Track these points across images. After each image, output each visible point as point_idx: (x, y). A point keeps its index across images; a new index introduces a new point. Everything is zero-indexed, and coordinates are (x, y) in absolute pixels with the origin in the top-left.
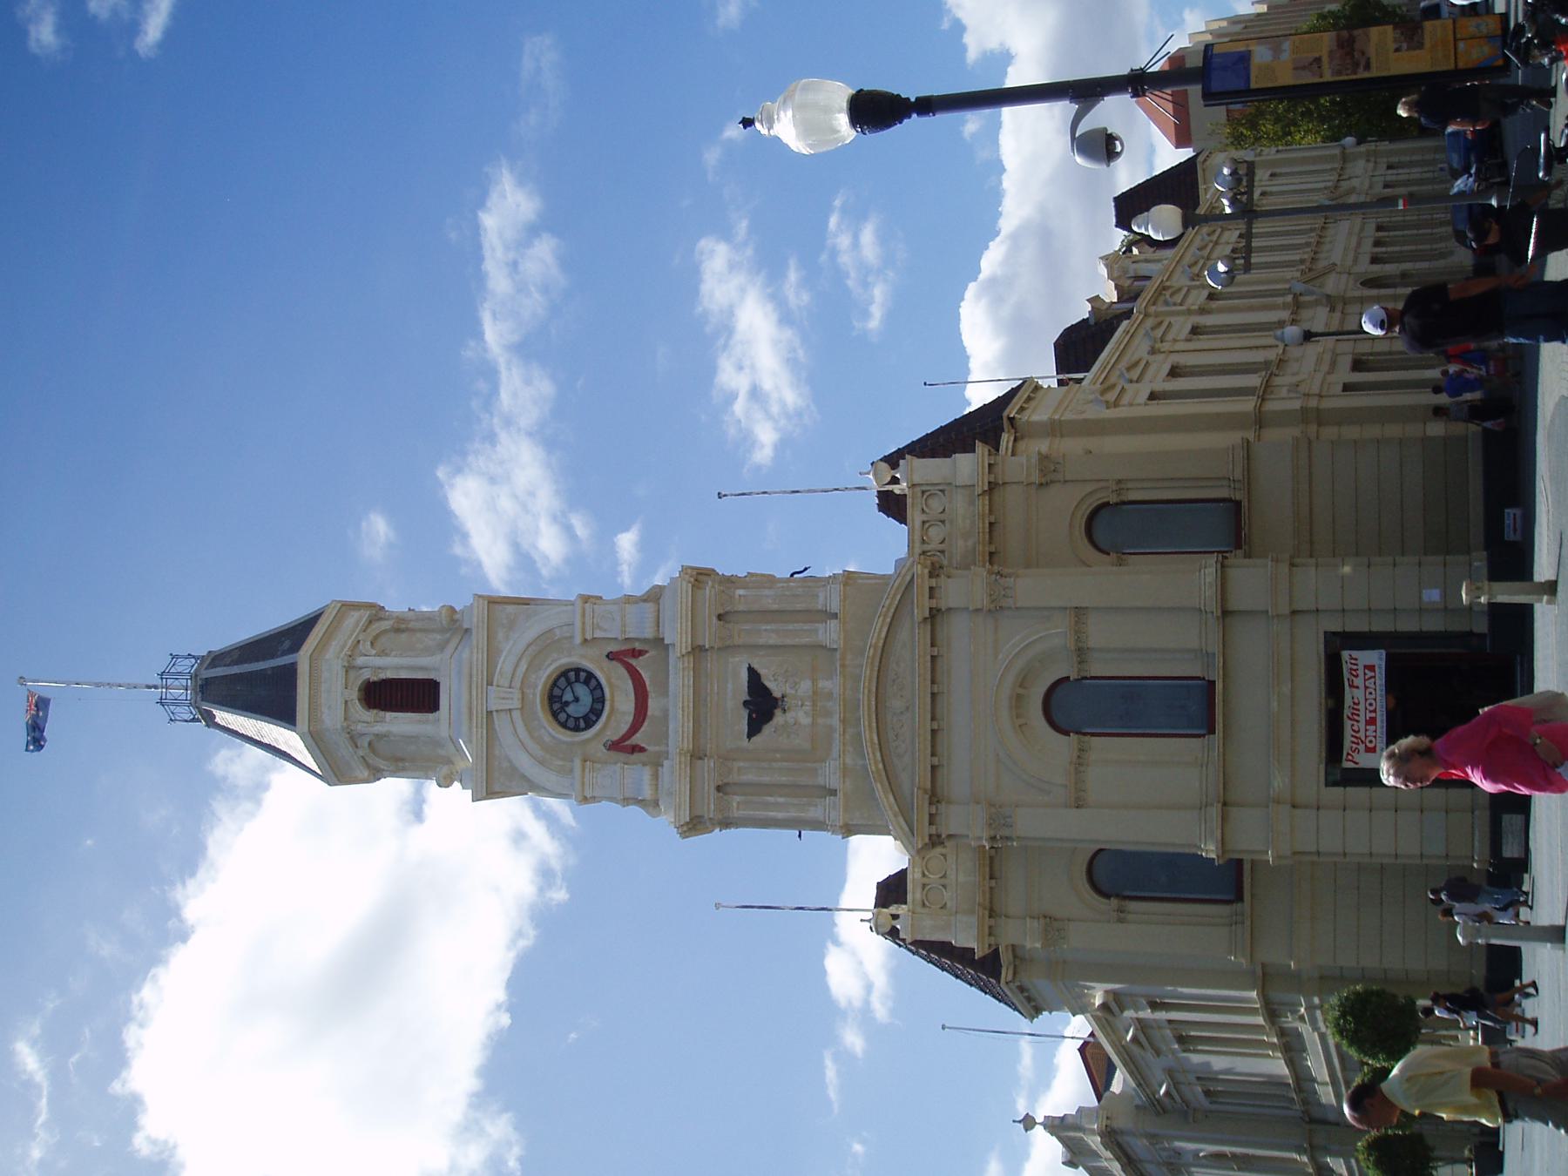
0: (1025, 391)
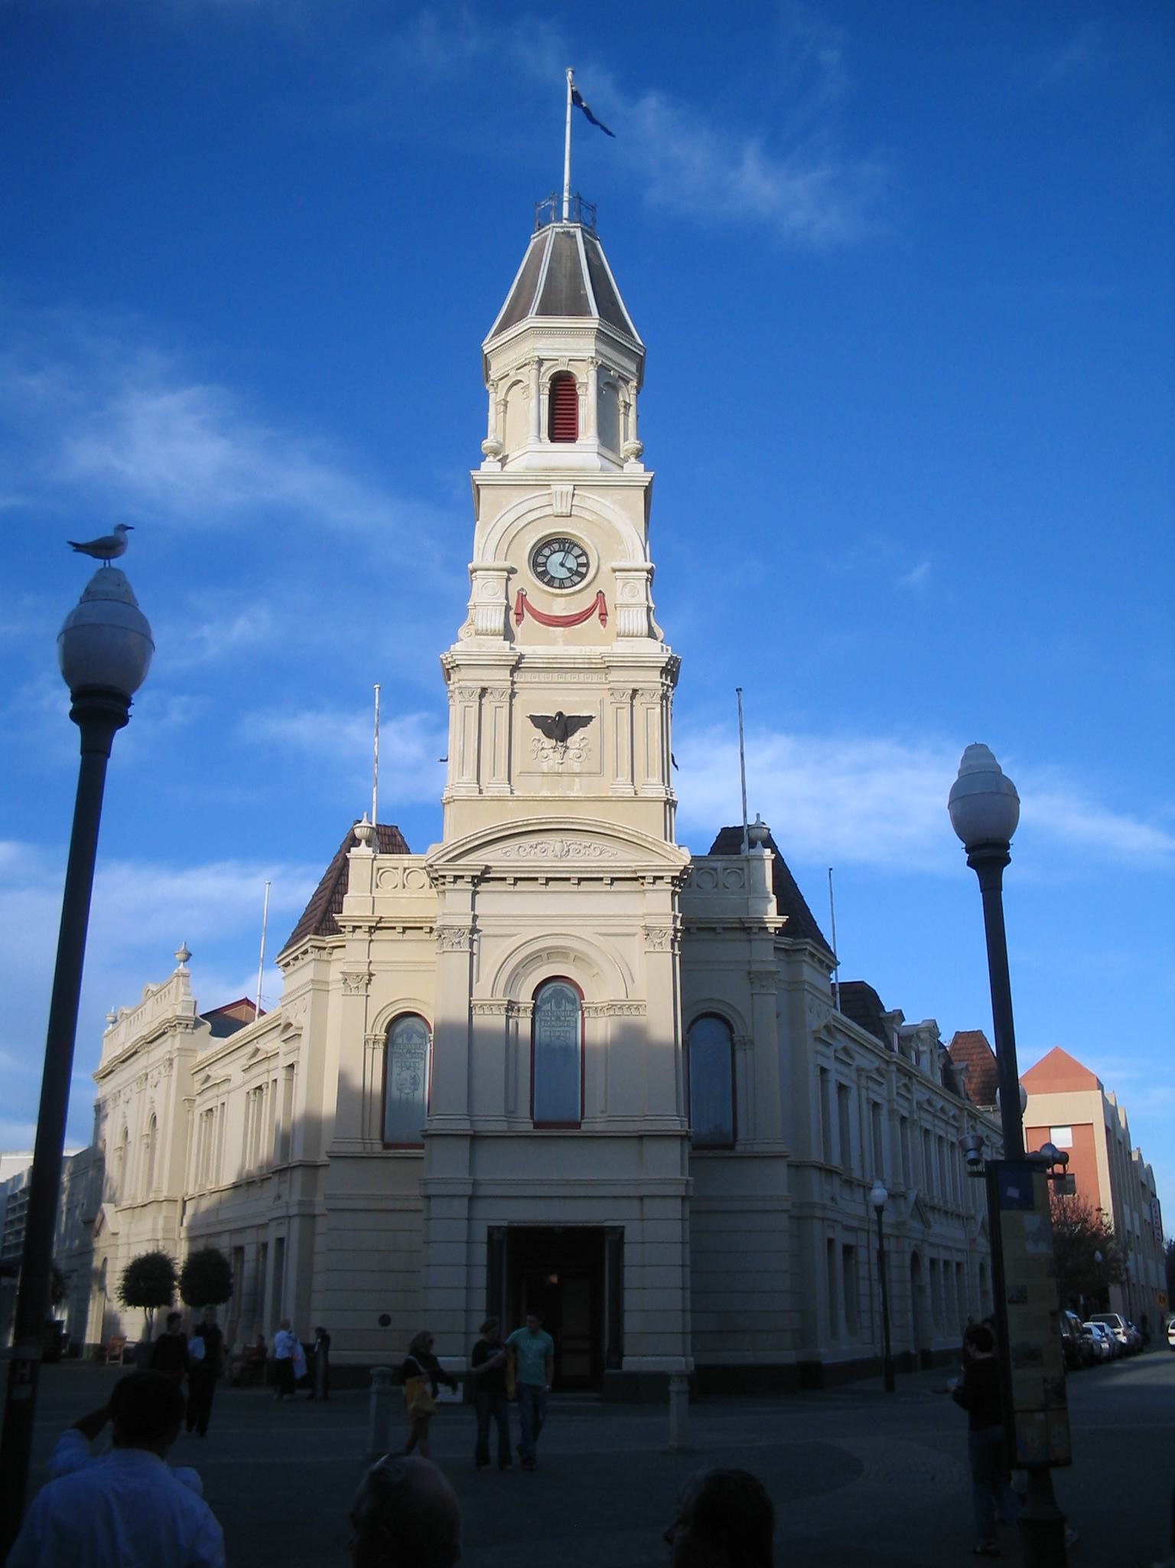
0: (827, 960)
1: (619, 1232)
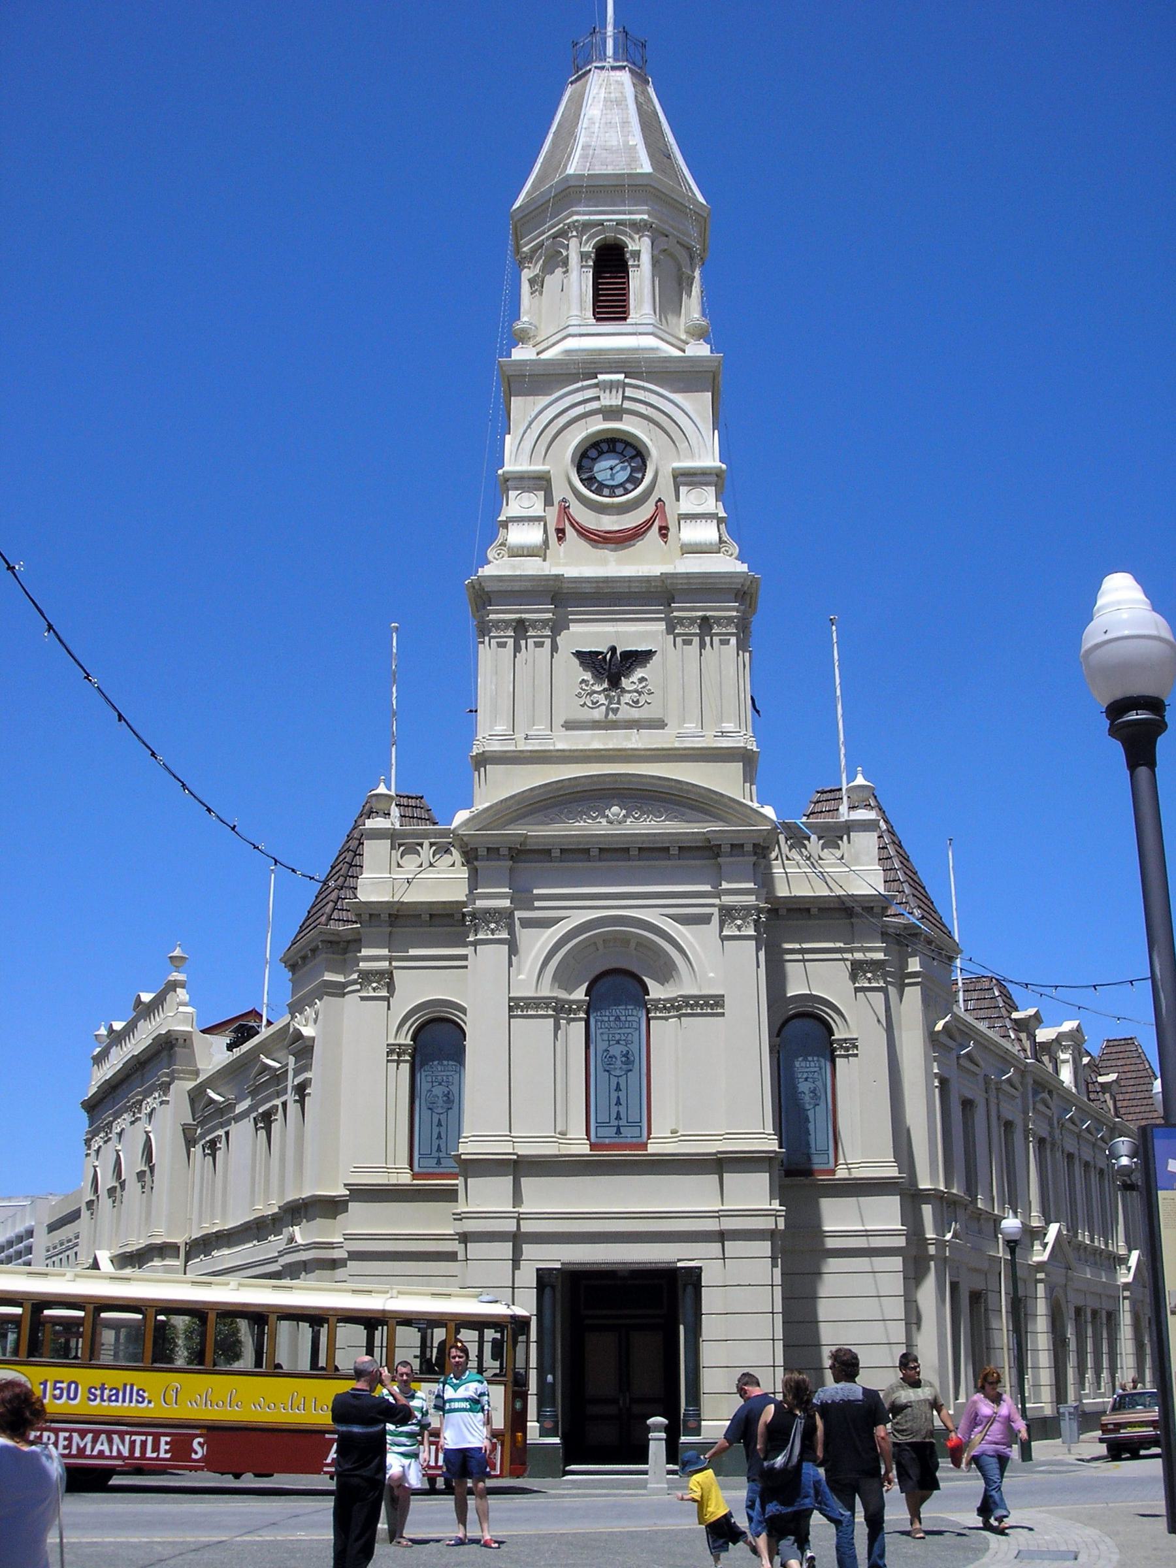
1: (695, 1274)
